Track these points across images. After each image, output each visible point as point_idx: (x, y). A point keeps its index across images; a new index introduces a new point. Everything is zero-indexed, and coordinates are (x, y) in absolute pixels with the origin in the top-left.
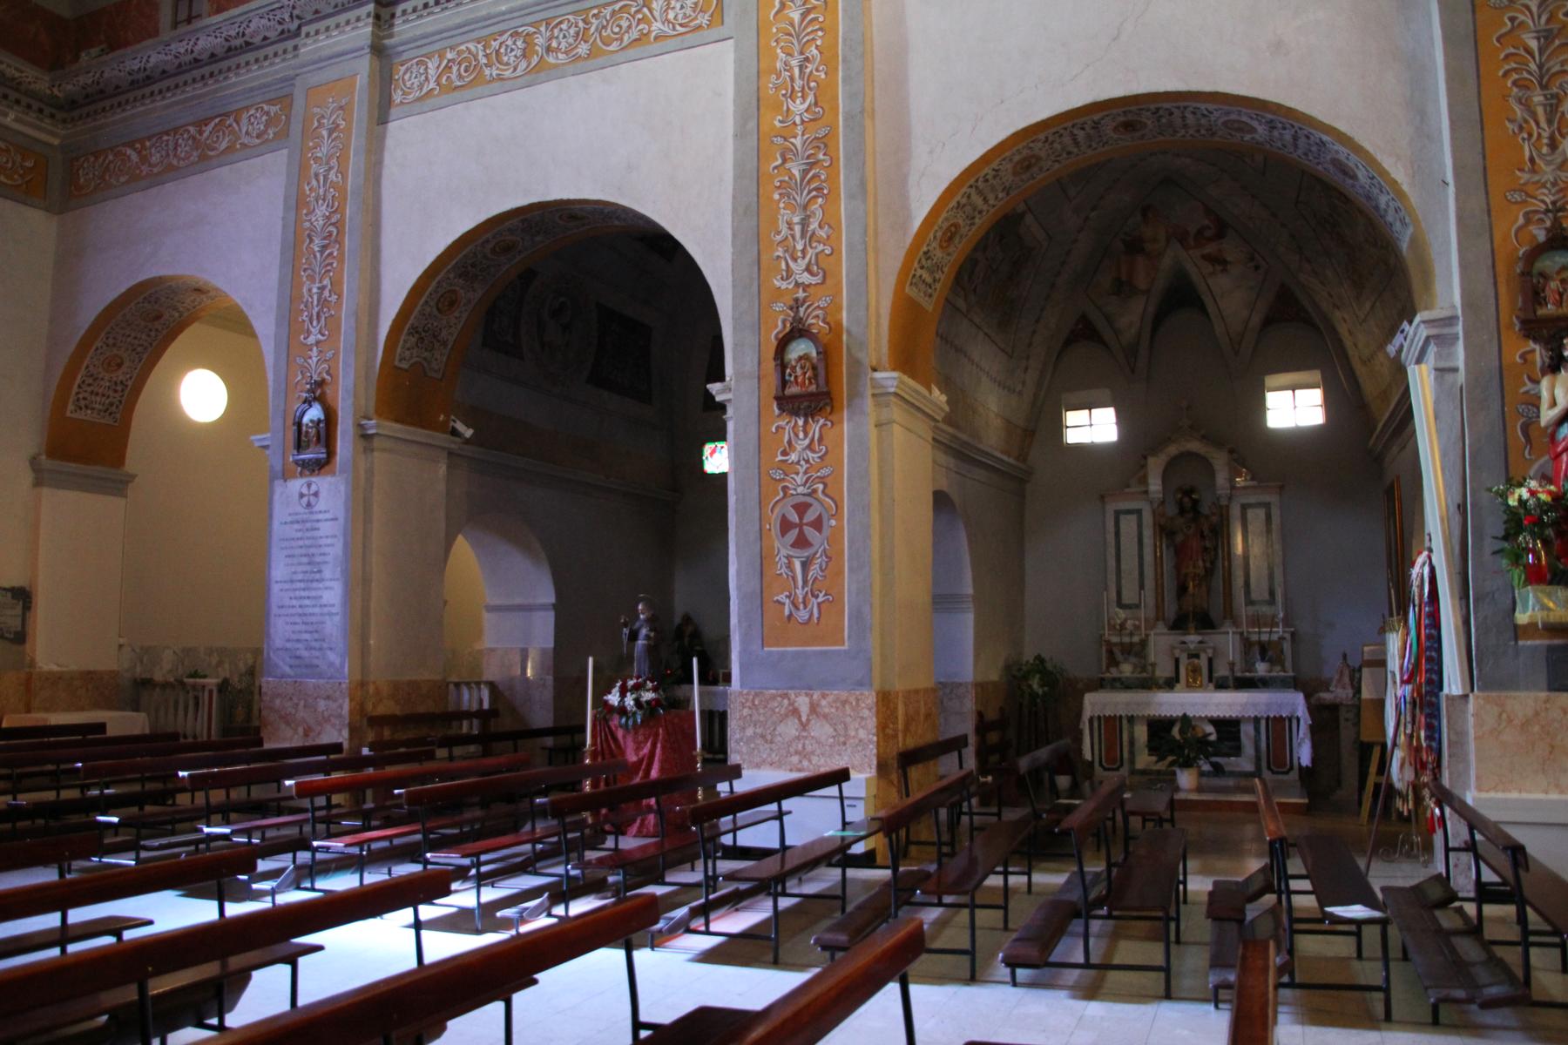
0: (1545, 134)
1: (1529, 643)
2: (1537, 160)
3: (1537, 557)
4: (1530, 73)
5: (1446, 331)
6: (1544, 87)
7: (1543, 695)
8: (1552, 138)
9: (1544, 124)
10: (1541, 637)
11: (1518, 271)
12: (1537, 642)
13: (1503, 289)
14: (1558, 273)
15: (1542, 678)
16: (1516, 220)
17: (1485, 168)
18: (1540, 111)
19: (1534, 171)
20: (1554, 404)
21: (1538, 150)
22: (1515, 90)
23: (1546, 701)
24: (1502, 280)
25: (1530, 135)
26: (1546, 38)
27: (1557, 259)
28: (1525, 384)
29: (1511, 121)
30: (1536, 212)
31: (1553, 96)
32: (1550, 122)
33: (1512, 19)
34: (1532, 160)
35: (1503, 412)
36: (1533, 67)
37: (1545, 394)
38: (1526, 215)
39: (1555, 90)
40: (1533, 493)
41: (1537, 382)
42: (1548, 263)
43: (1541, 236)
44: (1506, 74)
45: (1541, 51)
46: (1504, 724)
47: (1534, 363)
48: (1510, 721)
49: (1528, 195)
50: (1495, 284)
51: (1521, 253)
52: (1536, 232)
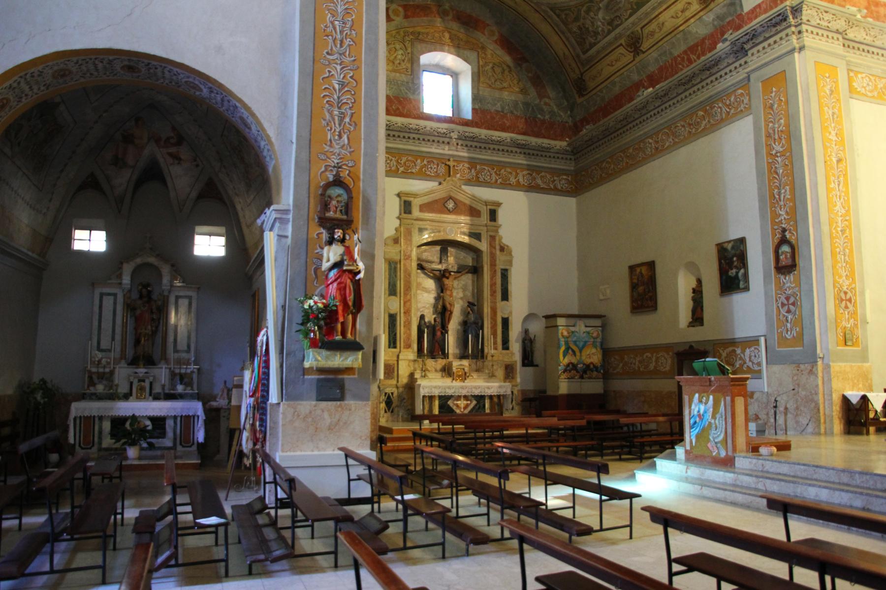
0: (338, 130)
1: (310, 377)
2: (333, 142)
3: (315, 335)
4: (334, 99)
5: (284, 216)
6: (339, 108)
7: (314, 403)
8: (340, 132)
10: (315, 374)
11: (320, 193)
12: (313, 377)
13: (312, 200)
14: (336, 197)
15: (314, 394)
16: (321, 168)
17: (310, 140)
18: (336, 118)
19: (331, 146)
20: (328, 260)
21: (334, 136)
22: (327, 105)
23: (315, 406)
24: (312, 195)
25: (331, 129)
26: (342, 85)
27: (337, 190)
28: (317, 249)
29: (325, 120)
30: (330, 166)
31: (343, 113)
32: (340, 125)
33: (329, 72)
34: (331, 140)
35: (306, 262)
36: (336, 97)
37: (325, 255)
38: (326, 166)
39: (343, 111)
40: (316, 303)
41: (322, 248)
42: (332, 192)
43: (331, 179)
44: (324, 96)
45: (340, 90)
46: (296, 417)
47: (322, 239)
48: (298, 416)
49: (327, 157)
50: (309, 197)
51: (322, 184)
52: (329, 176)
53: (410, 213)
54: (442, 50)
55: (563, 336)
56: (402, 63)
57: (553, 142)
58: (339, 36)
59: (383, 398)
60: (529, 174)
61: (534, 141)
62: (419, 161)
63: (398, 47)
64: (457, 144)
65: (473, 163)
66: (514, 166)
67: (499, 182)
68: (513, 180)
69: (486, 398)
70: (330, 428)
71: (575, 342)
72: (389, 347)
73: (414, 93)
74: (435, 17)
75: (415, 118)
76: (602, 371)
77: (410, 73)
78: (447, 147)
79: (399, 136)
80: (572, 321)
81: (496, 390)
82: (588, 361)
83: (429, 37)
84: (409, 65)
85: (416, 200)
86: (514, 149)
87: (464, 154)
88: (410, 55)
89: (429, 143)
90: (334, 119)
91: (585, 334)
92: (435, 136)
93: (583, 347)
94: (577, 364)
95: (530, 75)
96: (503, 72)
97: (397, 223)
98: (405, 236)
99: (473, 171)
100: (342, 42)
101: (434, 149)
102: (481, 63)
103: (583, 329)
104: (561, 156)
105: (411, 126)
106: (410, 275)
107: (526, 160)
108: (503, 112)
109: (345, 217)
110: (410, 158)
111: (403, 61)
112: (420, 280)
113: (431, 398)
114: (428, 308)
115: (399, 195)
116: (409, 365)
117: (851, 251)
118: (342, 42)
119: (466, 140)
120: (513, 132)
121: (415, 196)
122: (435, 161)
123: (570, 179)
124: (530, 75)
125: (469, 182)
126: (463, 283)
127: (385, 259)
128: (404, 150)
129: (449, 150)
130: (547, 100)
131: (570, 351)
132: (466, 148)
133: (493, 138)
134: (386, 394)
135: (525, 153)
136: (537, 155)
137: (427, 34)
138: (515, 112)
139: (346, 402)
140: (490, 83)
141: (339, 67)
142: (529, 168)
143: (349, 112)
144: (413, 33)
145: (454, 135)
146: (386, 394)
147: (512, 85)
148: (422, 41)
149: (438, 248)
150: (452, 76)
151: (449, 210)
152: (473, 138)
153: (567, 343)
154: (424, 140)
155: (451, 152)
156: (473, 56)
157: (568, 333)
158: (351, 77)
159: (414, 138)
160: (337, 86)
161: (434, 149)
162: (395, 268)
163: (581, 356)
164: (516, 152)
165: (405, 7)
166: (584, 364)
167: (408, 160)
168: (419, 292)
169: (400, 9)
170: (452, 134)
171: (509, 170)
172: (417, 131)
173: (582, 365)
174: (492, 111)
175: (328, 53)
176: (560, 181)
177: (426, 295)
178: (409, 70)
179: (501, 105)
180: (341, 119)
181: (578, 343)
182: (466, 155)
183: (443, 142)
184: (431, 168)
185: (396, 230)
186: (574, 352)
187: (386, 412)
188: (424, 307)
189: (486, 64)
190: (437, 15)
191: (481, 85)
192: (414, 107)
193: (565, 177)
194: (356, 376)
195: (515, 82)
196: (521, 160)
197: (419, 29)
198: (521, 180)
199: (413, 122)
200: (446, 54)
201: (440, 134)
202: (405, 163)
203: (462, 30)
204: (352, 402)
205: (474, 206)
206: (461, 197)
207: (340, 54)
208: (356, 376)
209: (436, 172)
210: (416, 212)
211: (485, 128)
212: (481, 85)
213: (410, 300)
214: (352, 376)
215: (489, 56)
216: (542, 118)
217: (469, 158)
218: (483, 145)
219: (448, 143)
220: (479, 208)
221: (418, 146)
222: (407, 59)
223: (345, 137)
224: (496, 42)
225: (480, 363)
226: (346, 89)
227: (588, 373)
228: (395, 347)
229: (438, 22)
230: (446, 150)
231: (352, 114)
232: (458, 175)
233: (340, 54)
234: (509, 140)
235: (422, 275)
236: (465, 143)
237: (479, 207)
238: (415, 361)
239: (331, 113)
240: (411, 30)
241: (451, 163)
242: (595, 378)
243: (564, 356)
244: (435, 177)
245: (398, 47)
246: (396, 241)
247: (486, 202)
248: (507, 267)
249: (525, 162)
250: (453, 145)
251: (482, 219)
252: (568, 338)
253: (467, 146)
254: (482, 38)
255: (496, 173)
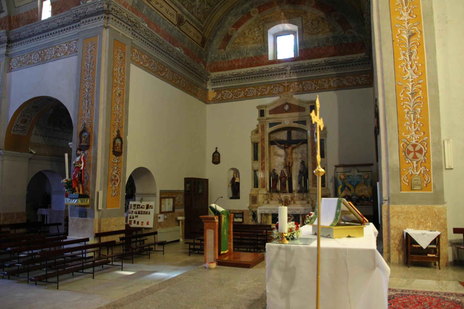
6: (88, 100)
7: (78, 218)
8: (87, 110)
9: (87, 107)
13: (78, 139)
15: (78, 214)
32: (87, 107)
33: (85, 86)
36: (87, 95)
45: (88, 92)
53: (263, 116)
54: (280, 23)
55: (341, 179)
56: (258, 37)
57: (354, 56)
58: (88, 70)
59: (251, 213)
60: (337, 79)
61: (340, 58)
62: (269, 87)
63: (256, 30)
64: (291, 73)
65: (300, 81)
66: (328, 77)
67: (317, 89)
68: (326, 86)
69: (300, 215)
70: (82, 228)
71: (350, 182)
72: (254, 188)
73: (265, 52)
74: (276, 6)
75: (266, 65)
76: (372, 201)
77: (262, 42)
78: (284, 76)
79: (258, 77)
80: (348, 169)
81: (302, 211)
82: (361, 194)
83: (273, 19)
84: (262, 38)
85: (267, 109)
86: (327, 67)
87: (295, 77)
88: (262, 32)
89: (274, 76)
90: (86, 105)
91: (358, 177)
92: (277, 71)
93: (357, 185)
94: (352, 196)
95: (337, 18)
96: (318, 23)
97: (257, 122)
98: (261, 128)
99: (300, 86)
100: (89, 71)
101: (277, 79)
102: (304, 22)
103: (356, 173)
104: (361, 63)
105: (264, 70)
106: (264, 149)
107: (336, 71)
108: (318, 47)
109: (86, 144)
110: (264, 87)
111: (259, 36)
112: (275, 150)
113: (266, 215)
114: (281, 165)
115: (258, 107)
116: (264, 197)
117: (425, 109)
118: (89, 71)
119: (296, 69)
120: (326, 57)
121: (266, 106)
122: (278, 85)
123: (368, 76)
124: (337, 18)
125: (298, 93)
126: (301, 149)
127: (251, 141)
128: (260, 83)
129: (285, 77)
130: (350, 30)
131: (346, 188)
132: (296, 74)
133: (313, 63)
134: (252, 211)
135: (334, 67)
136: (343, 66)
137: (271, 17)
138: (327, 44)
139: (87, 218)
140: (310, 32)
141: (88, 83)
142: (338, 76)
143: (91, 100)
144: (263, 20)
145: (288, 68)
146: (252, 211)
147: (324, 28)
148: (269, 22)
149: (286, 132)
150: (293, 34)
151: (286, 111)
152: (300, 67)
153: (343, 183)
154: (271, 75)
155: (286, 78)
156: (299, 20)
157: (345, 177)
158: (92, 86)
159: (266, 76)
160: (87, 91)
161: (277, 79)
162: (257, 146)
163: (355, 191)
164: (328, 68)
165: (259, 8)
166: (357, 196)
167: (262, 88)
168: (275, 157)
169: (257, 9)
170: (287, 68)
171: (323, 80)
172: (267, 71)
173: (355, 197)
174: (312, 48)
175: (85, 78)
176: (361, 79)
177: (279, 158)
178: (262, 40)
179: (317, 43)
180: (88, 104)
181: (352, 183)
182: (296, 77)
183: (282, 74)
184: (276, 89)
185: (257, 126)
186: (348, 188)
187: (252, 221)
188: (278, 165)
189: (307, 22)
190: (277, 5)
191: (304, 35)
192: (265, 59)
193: (364, 76)
194: (90, 208)
195: (327, 26)
196: (332, 72)
197: (267, 16)
198: (332, 84)
199: (265, 67)
200: (283, 24)
201: (280, 70)
202: (261, 90)
203: (292, 8)
204: (89, 218)
205: (301, 105)
206: (293, 102)
207: (89, 77)
208: (90, 208)
209: (278, 91)
210: (267, 115)
211: (307, 59)
212: (304, 35)
213: (264, 162)
214: (89, 208)
215: (309, 17)
216: (346, 42)
217: (298, 79)
218: (306, 70)
219: (285, 73)
220: (304, 106)
221: (268, 79)
222: (260, 35)
223: (89, 111)
224: (313, 7)
225: (305, 195)
226: (90, 91)
227: (360, 201)
228: (257, 187)
229: (277, 8)
230: (284, 78)
231: (92, 101)
232: (291, 90)
233: (89, 77)
234: (323, 62)
235: (277, 148)
236: (294, 71)
237: (304, 105)
238: (267, 194)
239: (85, 102)
240: (262, 19)
241: (286, 85)
242: (366, 205)
243: (342, 192)
244: (279, 93)
245: (256, 30)
246: (257, 132)
247: (307, 102)
248: (323, 138)
249: (335, 73)
250: (288, 73)
251: (306, 112)
252: (344, 180)
253: (296, 72)
254: (304, 7)
255: (315, 84)
